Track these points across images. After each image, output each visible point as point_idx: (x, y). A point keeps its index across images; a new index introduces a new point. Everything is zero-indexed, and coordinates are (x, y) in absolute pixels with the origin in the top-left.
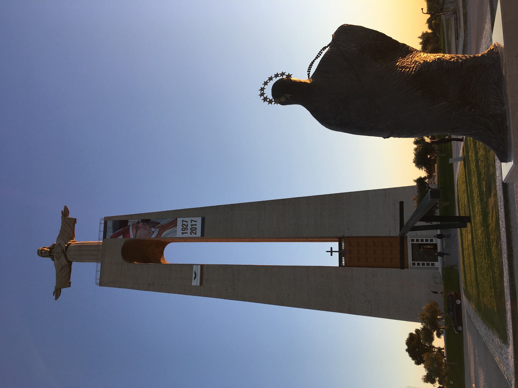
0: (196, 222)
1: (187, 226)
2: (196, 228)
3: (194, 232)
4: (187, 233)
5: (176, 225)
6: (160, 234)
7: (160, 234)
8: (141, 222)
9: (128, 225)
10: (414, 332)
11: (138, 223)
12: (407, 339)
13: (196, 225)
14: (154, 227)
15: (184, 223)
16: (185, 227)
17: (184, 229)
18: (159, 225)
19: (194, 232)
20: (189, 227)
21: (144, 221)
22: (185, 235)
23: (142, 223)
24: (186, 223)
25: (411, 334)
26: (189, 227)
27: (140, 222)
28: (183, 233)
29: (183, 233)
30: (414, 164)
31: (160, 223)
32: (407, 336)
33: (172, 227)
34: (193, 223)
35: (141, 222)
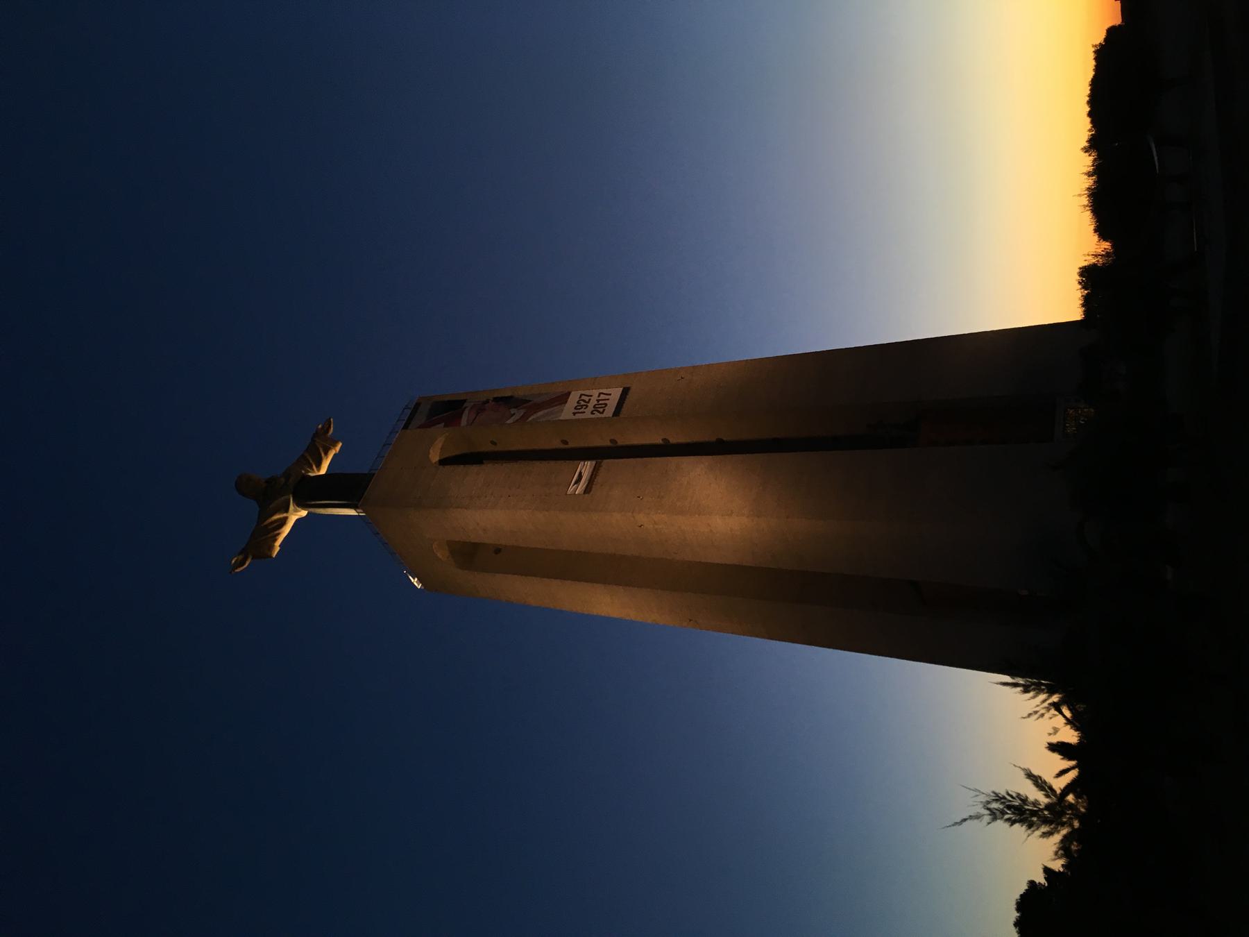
0: (610, 394)
1: (588, 402)
2: (606, 405)
3: (601, 410)
4: (584, 412)
5: (566, 402)
6: (524, 418)
7: (524, 418)
8: (493, 401)
9: (465, 405)
10: (1040, 879)
11: (487, 401)
12: (1021, 895)
13: (608, 399)
14: (516, 407)
15: (583, 397)
16: (582, 403)
17: (580, 406)
18: (531, 403)
19: (601, 410)
20: (593, 402)
21: (497, 400)
22: (578, 416)
23: (493, 403)
24: (587, 399)
25: (1032, 884)
26: (591, 406)
27: (490, 402)
28: (574, 414)
29: (574, 414)
30: (1078, 270)
31: (530, 401)
32: (1023, 887)
33: (556, 406)
34: (602, 397)
35: (493, 401)
